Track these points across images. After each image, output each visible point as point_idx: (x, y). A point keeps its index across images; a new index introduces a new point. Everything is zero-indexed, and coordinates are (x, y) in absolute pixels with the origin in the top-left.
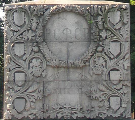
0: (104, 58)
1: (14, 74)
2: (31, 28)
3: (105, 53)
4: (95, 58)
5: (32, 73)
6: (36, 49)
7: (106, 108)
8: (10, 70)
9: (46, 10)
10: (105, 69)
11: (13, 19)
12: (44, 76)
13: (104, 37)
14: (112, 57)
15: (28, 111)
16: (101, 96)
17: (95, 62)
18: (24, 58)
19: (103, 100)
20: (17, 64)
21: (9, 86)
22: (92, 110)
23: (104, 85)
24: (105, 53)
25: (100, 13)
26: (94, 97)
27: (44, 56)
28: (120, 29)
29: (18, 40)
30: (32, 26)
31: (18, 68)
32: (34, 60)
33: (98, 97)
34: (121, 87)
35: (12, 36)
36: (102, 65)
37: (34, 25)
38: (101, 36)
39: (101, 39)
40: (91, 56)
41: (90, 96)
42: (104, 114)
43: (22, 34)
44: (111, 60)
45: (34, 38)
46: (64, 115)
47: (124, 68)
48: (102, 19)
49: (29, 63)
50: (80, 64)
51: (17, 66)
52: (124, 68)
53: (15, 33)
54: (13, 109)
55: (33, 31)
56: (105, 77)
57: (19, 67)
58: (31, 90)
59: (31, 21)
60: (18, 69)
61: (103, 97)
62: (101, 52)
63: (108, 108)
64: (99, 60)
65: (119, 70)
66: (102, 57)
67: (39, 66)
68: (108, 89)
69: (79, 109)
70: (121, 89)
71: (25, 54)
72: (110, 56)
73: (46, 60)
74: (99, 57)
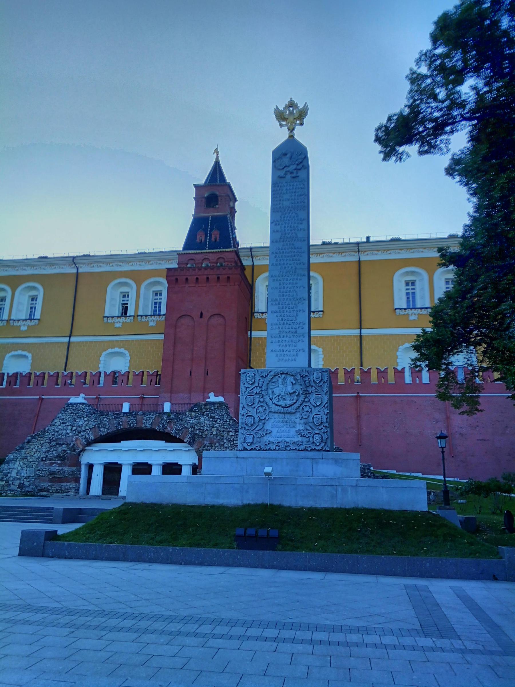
2: (258, 385)
3: (311, 403)
5: (258, 417)
6: (262, 400)
8: (243, 415)
9: (269, 372)
10: (310, 414)
12: (267, 419)
14: (316, 405)
15: (256, 443)
17: (303, 409)
18: (253, 406)
19: (309, 437)
20: (248, 411)
22: (301, 444)
24: (311, 403)
25: (307, 374)
26: (303, 435)
28: (321, 386)
32: (260, 407)
40: (301, 405)
42: (310, 447)
43: (252, 389)
45: (260, 392)
48: (309, 379)
51: (249, 412)
53: (248, 389)
55: (260, 387)
58: (257, 429)
61: (309, 435)
62: (307, 402)
68: (312, 429)
73: (269, 408)
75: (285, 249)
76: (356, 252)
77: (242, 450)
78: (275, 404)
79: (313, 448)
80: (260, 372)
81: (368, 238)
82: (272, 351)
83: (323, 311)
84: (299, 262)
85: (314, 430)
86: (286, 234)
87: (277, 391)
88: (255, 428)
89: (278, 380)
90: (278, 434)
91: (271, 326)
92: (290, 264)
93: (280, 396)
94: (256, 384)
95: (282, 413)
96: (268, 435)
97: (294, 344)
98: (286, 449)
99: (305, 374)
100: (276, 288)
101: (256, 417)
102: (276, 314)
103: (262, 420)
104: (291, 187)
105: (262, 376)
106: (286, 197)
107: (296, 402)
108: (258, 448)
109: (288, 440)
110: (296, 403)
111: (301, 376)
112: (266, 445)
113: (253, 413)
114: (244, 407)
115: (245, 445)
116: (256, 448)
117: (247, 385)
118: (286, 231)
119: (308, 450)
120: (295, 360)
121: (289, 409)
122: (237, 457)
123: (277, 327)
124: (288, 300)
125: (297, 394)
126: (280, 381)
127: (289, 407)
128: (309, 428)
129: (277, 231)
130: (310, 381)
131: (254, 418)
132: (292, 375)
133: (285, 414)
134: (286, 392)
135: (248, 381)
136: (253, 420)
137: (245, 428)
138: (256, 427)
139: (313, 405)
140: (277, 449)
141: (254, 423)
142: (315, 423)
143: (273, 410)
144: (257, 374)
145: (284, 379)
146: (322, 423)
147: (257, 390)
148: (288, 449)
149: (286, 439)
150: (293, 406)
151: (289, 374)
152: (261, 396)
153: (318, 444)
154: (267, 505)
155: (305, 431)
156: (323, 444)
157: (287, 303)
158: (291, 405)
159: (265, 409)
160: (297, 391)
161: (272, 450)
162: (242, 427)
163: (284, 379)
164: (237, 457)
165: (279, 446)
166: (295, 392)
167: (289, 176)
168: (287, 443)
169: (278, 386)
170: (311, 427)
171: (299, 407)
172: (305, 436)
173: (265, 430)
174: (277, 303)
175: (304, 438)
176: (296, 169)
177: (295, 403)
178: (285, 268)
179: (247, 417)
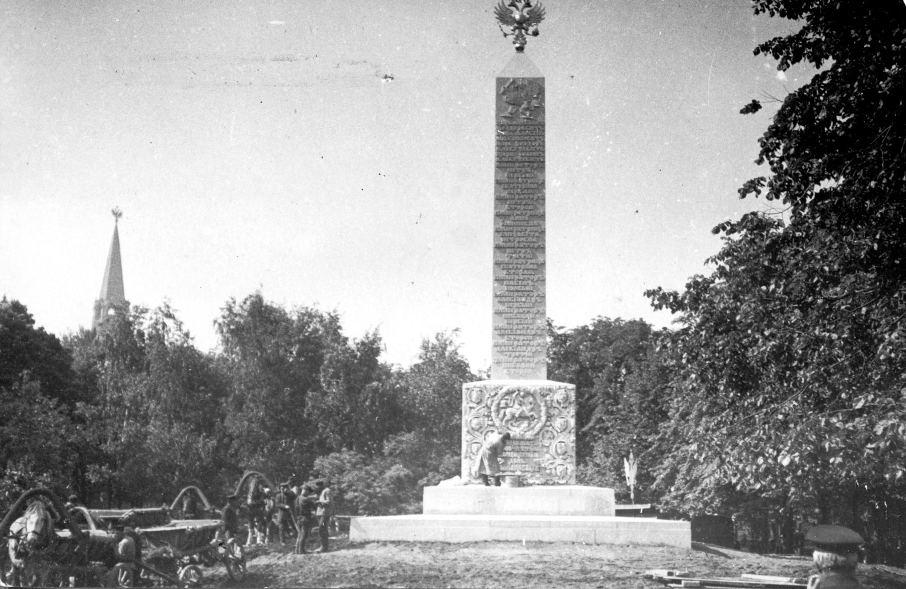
10: (552, 441)
17: (543, 435)
18: (480, 431)
37: (489, 402)
60: (474, 441)
74: (547, 431)
137: (470, 457)
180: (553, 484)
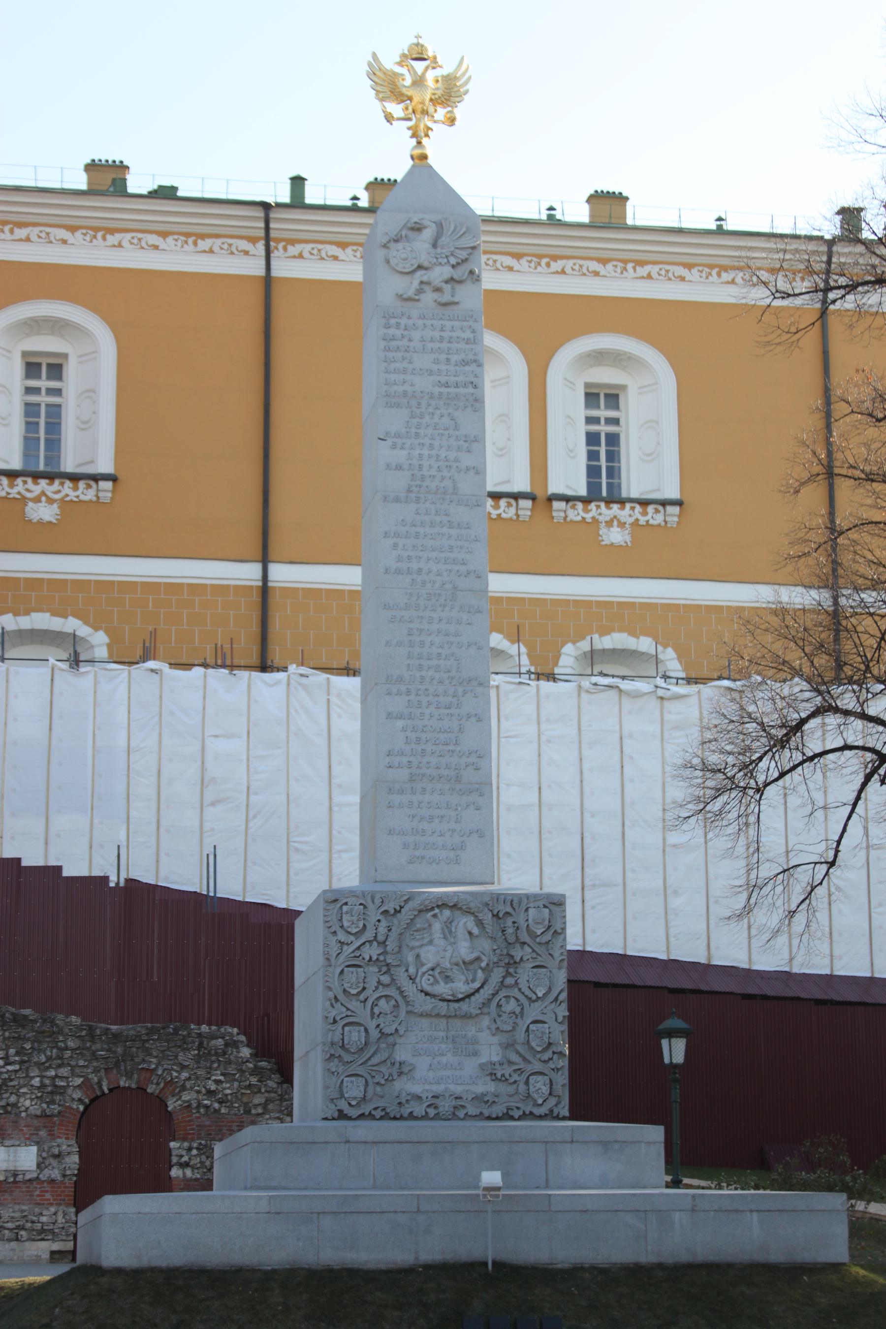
0: (517, 1000)
1: (343, 1028)
2: (375, 937)
3: (520, 989)
4: (501, 1000)
5: (378, 1026)
6: (386, 979)
7: (522, 1097)
8: (335, 1021)
9: (406, 901)
10: (519, 1021)
11: (339, 920)
12: (401, 1032)
13: (518, 959)
14: (534, 997)
15: (371, 1100)
16: (512, 1074)
17: (499, 1006)
18: (362, 997)
19: (515, 1082)
20: (348, 1009)
21: (333, 1052)
22: (494, 1102)
23: (518, 1053)
24: (520, 989)
25: (509, 909)
26: (499, 1076)
27: (401, 992)
28: (547, 943)
29: (351, 960)
30: (378, 934)
31: (351, 1016)
32: (382, 1002)
33: (507, 1076)
34: (551, 1057)
35: (339, 954)
36: (514, 1013)
37: (382, 930)
38: (512, 957)
39: (512, 962)
40: (494, 995)
41: (491, 1074)
42: (518, 1108)
43: (358, 948)
44: (532, 1004)
45: (381, 958)
46: (441, 1109)
47: (556, 1020)
48: (514, 922)
49: (372, 1009)
50: (472, 1011)
51: (349, 1013)
52: (556, 1020)
53: (345, 947)
54: (341, 1098)
55: (379, 943)
56: (520, 1036)
57: (352, 1014)
58: (375, 1060)
59: (377, 923)
61: (515, 1077)
63: (525, 1098)
64: (508, 1003)
65: (544, 1023)
66: (513, 997)
67: (392, 1013)
68: (525, 1059)
69: (470, 1099)
70: (551, 1062)
71: (364, 988)
72: (530, 996)
73: (407, 1003)
74: (507, 997)
75: (423, 524)
76: (253, 240)
77: (333, 1119)
78: (422, 991)
79: (527, 1113)
80: (378, 901)
81: (298, 182)
82: (391, 832)
83: (113, 478)
84: (463, 569)
85: (529, 1062)
86: (423, 478)
87: (430, 956)
88: (369, 1059)
89: (430, 925)
90: (431, 1074)
91: (388, 759)
92: (439, 574)
93: (438, 971)
94: (369, 935)
95: (445, 1016)
96: (404, 1078)
97: (453, 814)
98: (454, 1114)
99: (503, 909)
100: (399, 644)
101: (372, 1025)
102: (400, 723)
103: (388, 1035)
104: (437, 334)
105: (386, 912)
106: (423, 361)
107: (482, 986)
108: (378, 1114)
109: (458, 1090)
110: (482, 991)
111: (493, 915)
112: (400, 1103)
113: (363, 1014)
114: (336, 998)
115: (343, 1105)
116: (373, 1113)
117: (342, 936)
118: (425, 472)
119: (512, 1118)
120: (457, 861)
121: (464, 1006)
122: (348, 1142)
123: (405, 760)
124: (435, 682)
125: (483, 965)
126: (437, 926)
127: (462, 999)
128: (514, 1058)
129: (399, 468)
130: (518, 928)
131: (366, 1030)
132: (469, 912)
133: (450, 1020)
134: (454, 960)
135: (346, 924)
136: (363, 1034)
138: (372, 1056)
139: (526, 996)
140: (432, 1115)
141: (365, 1044)
142: (533, 1044)
143: (418, 1009)
144: (370, 906)
145: (449, 923)
146: (550, 1044)
147: (373, 951)
148: (461, 1114)
149: (452, 1087)
150: (473, 998)
151: (460, 909)
152: (384, 969)
153: (540, 1101)
154: (485, 1264)
155: (506, 1066)
156: (552, 1102)
157: (431, 691)
158: (469, 996)
159: (396, 1006)
160: (483, 957)
161: (416, 1118)
162: (332, 1055)
163: (449, 923)
164: (348, 1142)
165: (436, 1108)
166: (478, 959)
167: (429, 297)
168: (456, 1098)
169: (431, 942)
170: (521, 1055)
171: (490, 1000)
172: (507, 1080)
173: (397, 1065)
174: (403, 688)
175: (501, 1084)
176: (451, 280)
177: (478, 990)
178: (424, 583)
179: (346, 1029)
180: (523, 1117)
